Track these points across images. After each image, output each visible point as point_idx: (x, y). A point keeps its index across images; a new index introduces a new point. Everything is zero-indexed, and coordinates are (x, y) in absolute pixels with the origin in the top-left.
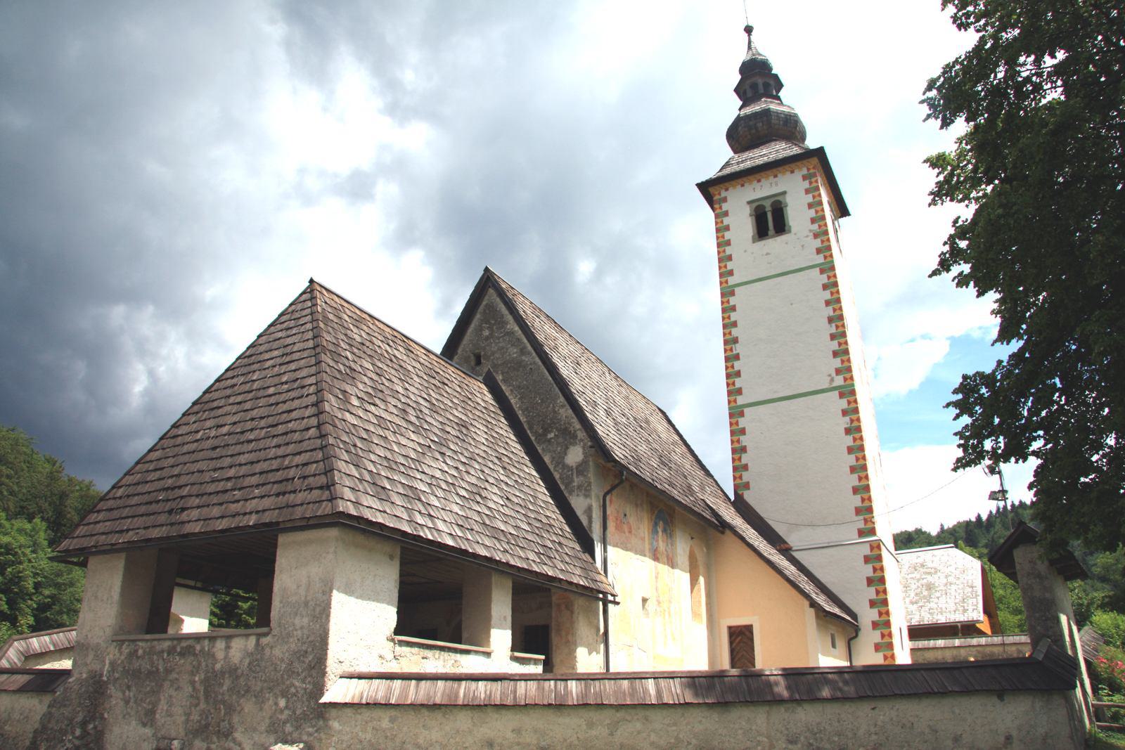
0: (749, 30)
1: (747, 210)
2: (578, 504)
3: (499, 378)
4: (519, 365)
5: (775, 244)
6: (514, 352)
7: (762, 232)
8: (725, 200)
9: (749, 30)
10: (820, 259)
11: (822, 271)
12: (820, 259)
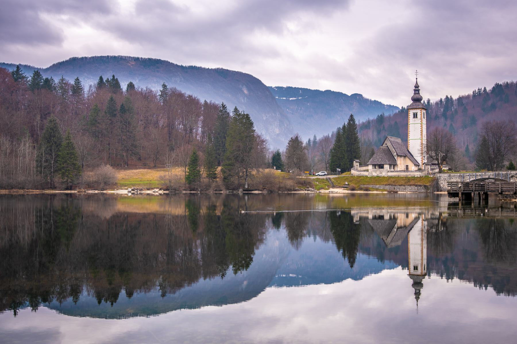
0: (417, 79)
1: (413, 114)
2: (395, 158)
3: (388, 146)
4: (390, 146)
5: (415, 119)
6: (390, 144)
7: (414, 117)
8: (410, 111)
9: (417, 79)
10: (420, 122)
11: (421, 124)
12: (420, 122)
